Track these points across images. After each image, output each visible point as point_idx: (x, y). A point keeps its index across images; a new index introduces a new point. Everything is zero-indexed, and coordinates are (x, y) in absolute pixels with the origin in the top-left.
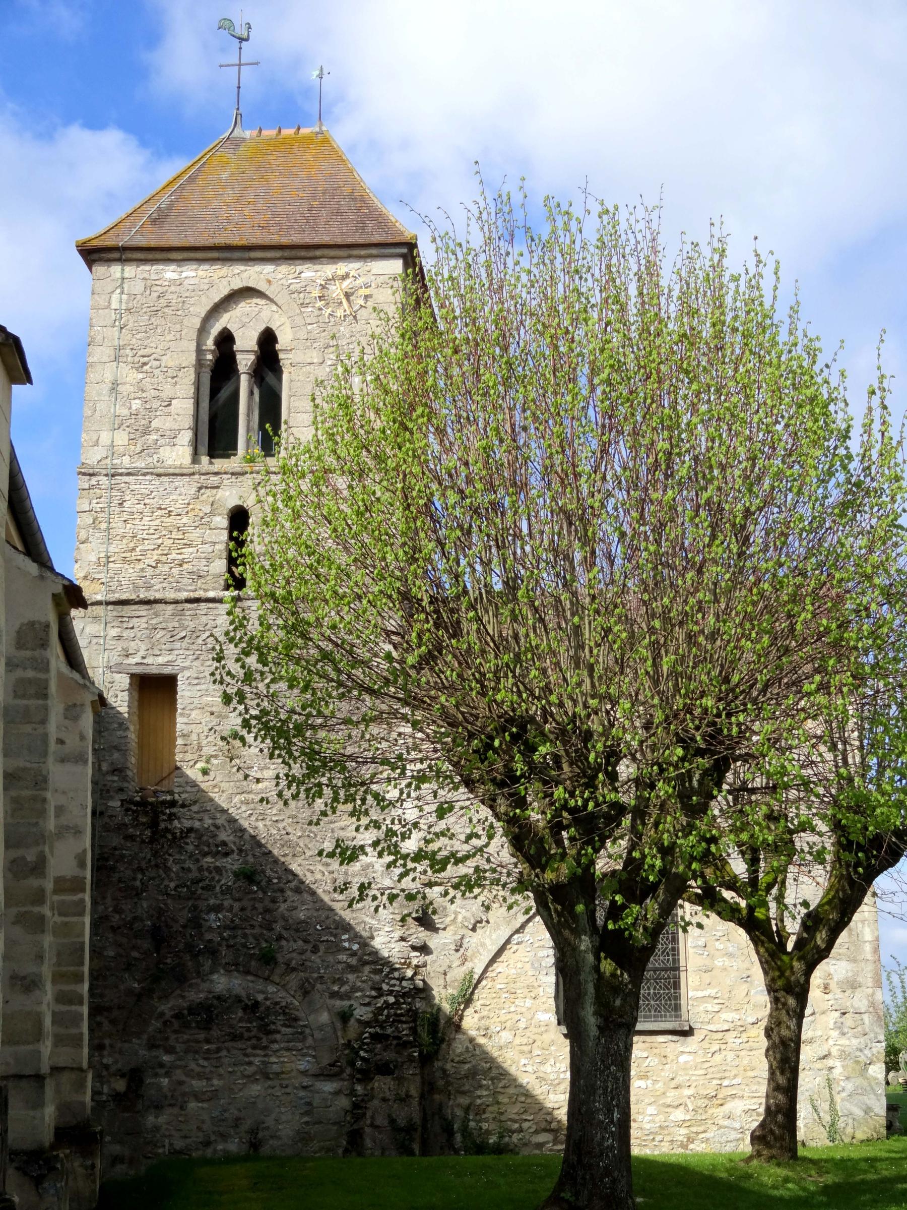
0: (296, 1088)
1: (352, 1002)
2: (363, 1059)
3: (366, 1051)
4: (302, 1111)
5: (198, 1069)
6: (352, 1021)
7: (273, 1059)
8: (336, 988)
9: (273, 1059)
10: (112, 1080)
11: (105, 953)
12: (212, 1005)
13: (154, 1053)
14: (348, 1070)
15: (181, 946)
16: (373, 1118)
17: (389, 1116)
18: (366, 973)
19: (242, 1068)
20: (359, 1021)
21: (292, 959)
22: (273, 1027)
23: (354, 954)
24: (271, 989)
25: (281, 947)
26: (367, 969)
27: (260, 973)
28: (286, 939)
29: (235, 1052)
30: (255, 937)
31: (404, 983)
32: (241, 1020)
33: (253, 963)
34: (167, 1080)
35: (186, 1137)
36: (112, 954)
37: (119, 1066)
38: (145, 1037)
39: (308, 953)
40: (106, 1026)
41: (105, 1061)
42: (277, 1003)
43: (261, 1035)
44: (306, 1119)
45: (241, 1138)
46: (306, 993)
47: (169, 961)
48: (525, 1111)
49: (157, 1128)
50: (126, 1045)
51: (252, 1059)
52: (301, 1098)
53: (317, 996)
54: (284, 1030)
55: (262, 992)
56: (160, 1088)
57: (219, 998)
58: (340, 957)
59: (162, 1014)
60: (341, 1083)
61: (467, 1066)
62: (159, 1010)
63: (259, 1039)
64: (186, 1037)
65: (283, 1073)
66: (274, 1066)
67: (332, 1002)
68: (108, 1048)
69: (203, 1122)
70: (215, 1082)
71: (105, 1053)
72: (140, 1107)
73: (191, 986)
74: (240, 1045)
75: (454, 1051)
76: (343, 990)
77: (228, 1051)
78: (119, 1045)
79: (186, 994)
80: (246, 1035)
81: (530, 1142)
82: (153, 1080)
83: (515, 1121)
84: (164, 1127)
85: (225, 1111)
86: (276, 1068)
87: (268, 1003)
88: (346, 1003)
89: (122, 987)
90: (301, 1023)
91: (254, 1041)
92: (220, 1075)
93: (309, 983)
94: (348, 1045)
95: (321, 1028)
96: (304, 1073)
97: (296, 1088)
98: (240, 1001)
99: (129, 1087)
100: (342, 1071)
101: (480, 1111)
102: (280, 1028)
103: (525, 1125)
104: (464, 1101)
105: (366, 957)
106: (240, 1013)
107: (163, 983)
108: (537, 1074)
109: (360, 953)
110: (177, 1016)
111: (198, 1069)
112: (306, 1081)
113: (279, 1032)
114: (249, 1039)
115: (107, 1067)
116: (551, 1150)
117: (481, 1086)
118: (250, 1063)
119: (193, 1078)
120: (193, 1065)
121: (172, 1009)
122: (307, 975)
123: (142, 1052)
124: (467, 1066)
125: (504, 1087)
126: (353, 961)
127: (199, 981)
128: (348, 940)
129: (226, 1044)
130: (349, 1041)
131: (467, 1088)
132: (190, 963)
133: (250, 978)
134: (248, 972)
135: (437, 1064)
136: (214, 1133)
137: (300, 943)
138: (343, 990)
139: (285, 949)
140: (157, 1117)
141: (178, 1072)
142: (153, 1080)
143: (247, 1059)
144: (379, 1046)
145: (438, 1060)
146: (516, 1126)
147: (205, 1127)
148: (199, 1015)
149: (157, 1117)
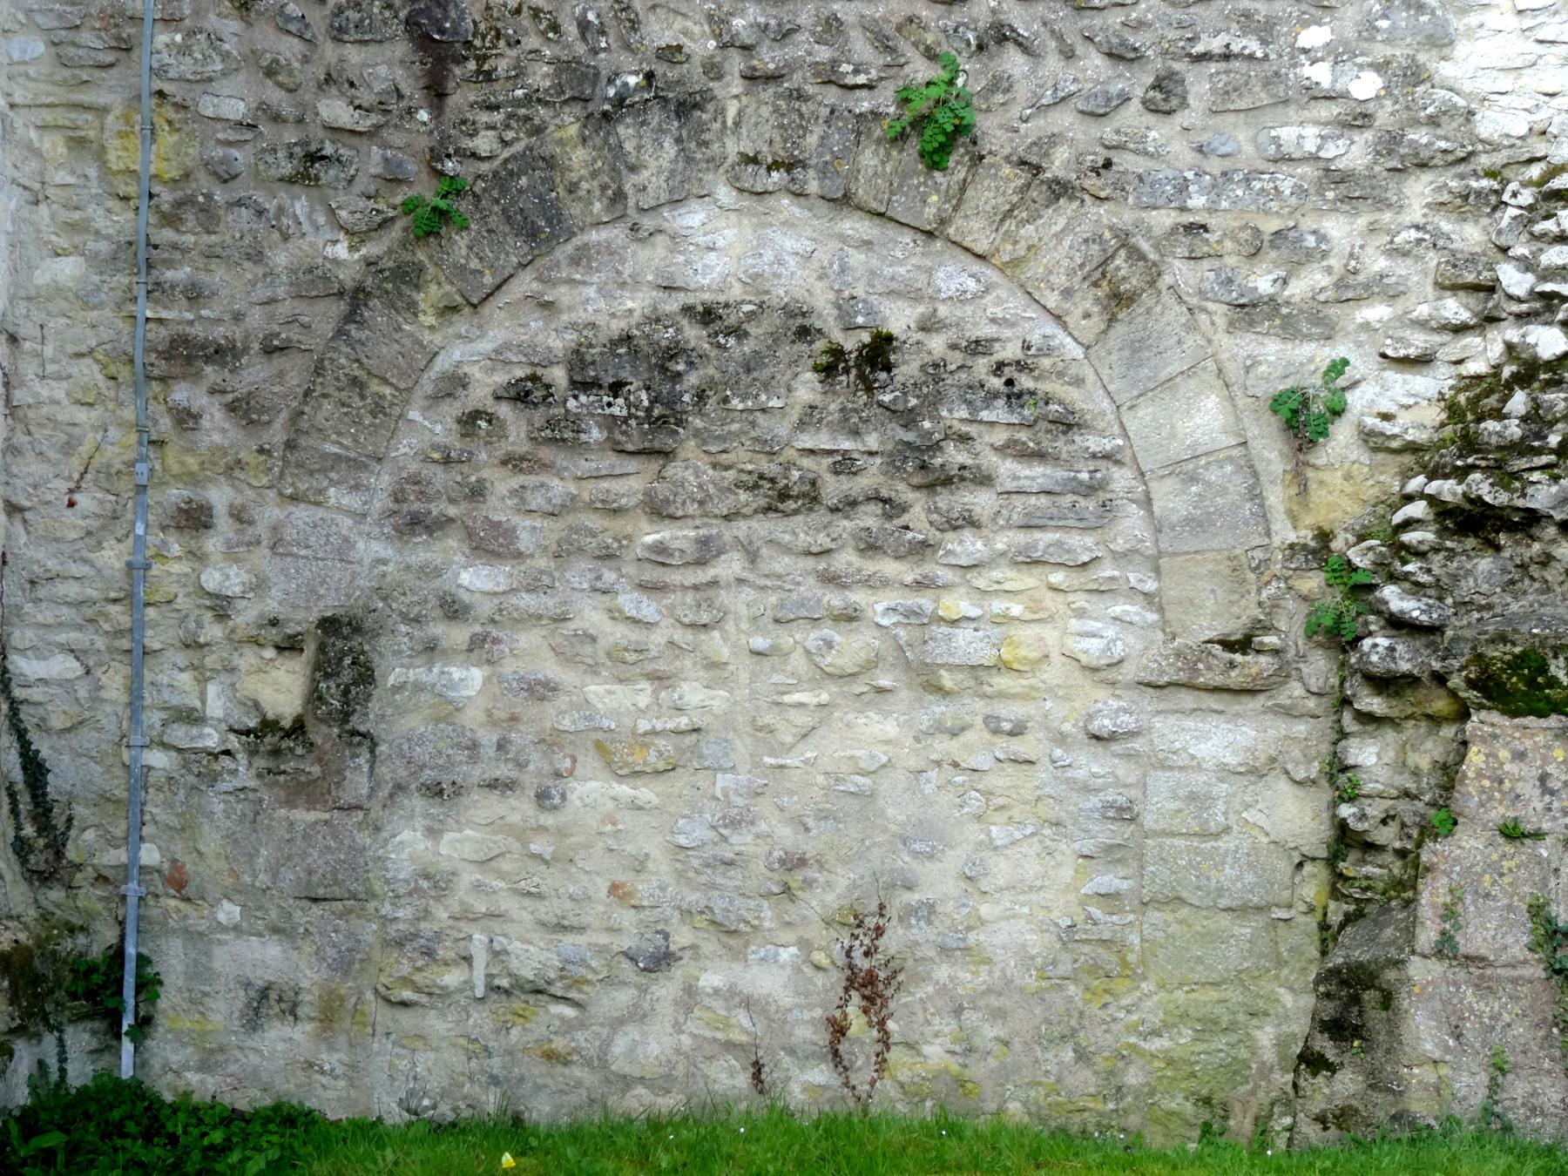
0: (1061, 739)
1: (1340, 350)
2: (1398, 624)
3: (1418, 588)
4: (1088, 846)
5: (619, 633)
6: (1342, 434)
7: (957, 604)
8: (1263, 283)
9: (957, 604)
10: (247, 659)
11: (208, 107)
12: (673, 352)
13: (423, 552)
14: (1319, 667)
15: (540, 76)
16: (1449, 913)
17: (1537, 911)
18: (1416, 213)
19: (812, 638)
20: (1373, 441)
21: (1054, 139)
22: (954, 456)
23: (1359, 119)
24: (953, 277)
25: (1000, 84)
26: (1419, 191)
27: (898, 212)
28: (1024, 47)
29: (782, 564)
30: (884, 45)
32: (810, 418)
33: (869, 158)
34: (477, 675)
35: (562, 928)
36: (236, 109)
37: (272, 604)
38: (382, 481)
39: (1132, 116)
40: (217, 427)
41: (212, 580)
42: (977, 347)
43: (906, 495)
44: (1107, 881)
45: (805, 945)
46: (1119, 300)
47: (484, 143)
49: (435, 882)
50: (302, 513)
51: (858, 597)
52: (1087, 789)
53: (1174, 314)
54: (1008, 470)
55: (914, 296)
56: (447, 710)
57: (707, 316)
58: (1287, 134)
59: (456, 383)
60: (1279, 728)
62: (442, 364)
63: (891, 507)
64: (559, 488)
65: (1002, 667)
66: (963, 636)
67: (1237, 347)
68: (223, 522)
69: (640, 865)
70: (693, 693)
71: (212, 544)
72: (357, 783)
73: (580, 258)
74: (800, 530)
76: (1298, 289)
77: (753, 557)
78: (270, 512)
79: (562, 294)
80: (833, 488)
82: (417, 673)
84: (468, 877)
85: (735, 824)
86: (968, 645)
87: (937, 344)
88: (1312, 356)
89: (280, 258)
90: (1094, 443)
91: (869, 518)
92: (714, 665)
93: (1136, 255)
94: (1320, 549)
95: (1185, 470)
96: (1101, 672)
97: (1061, 739)
98: (804, 333)
99: (315, 697)
100: (1283, 675)
102: (990, 460)
105: (1421, 136)
106: (807, 388)
107: (461, 241)
109: (1384, 117)
110: (521, 394)
111: (619, 633)
112: (1110, 712)
113: (984, 480)
114: (849, 505)
115: (221, 606)
118: (849, 617)
119: (593, 669)
120: (591, 616)
121: (497, 358)
122: (1126, 217)
123: (373, 548)
126: (1354, 153)
127: (616, 234)
128: (1338, 54)
129: (741, 528)
130: (1324, 537)
132: (579, 157)
133: (855, 226)
134: (844, 201)
136: (686, 914)
137: (1094, 63)
138: (1298, 289)
139: (1022, 92)
140: (433, 833)
141: (528, 639)
142: (417, 673)
143: (835, 599)
144: (1485, 564)
147: (644, 888)
148: (616, 388)
149: (433, 833)
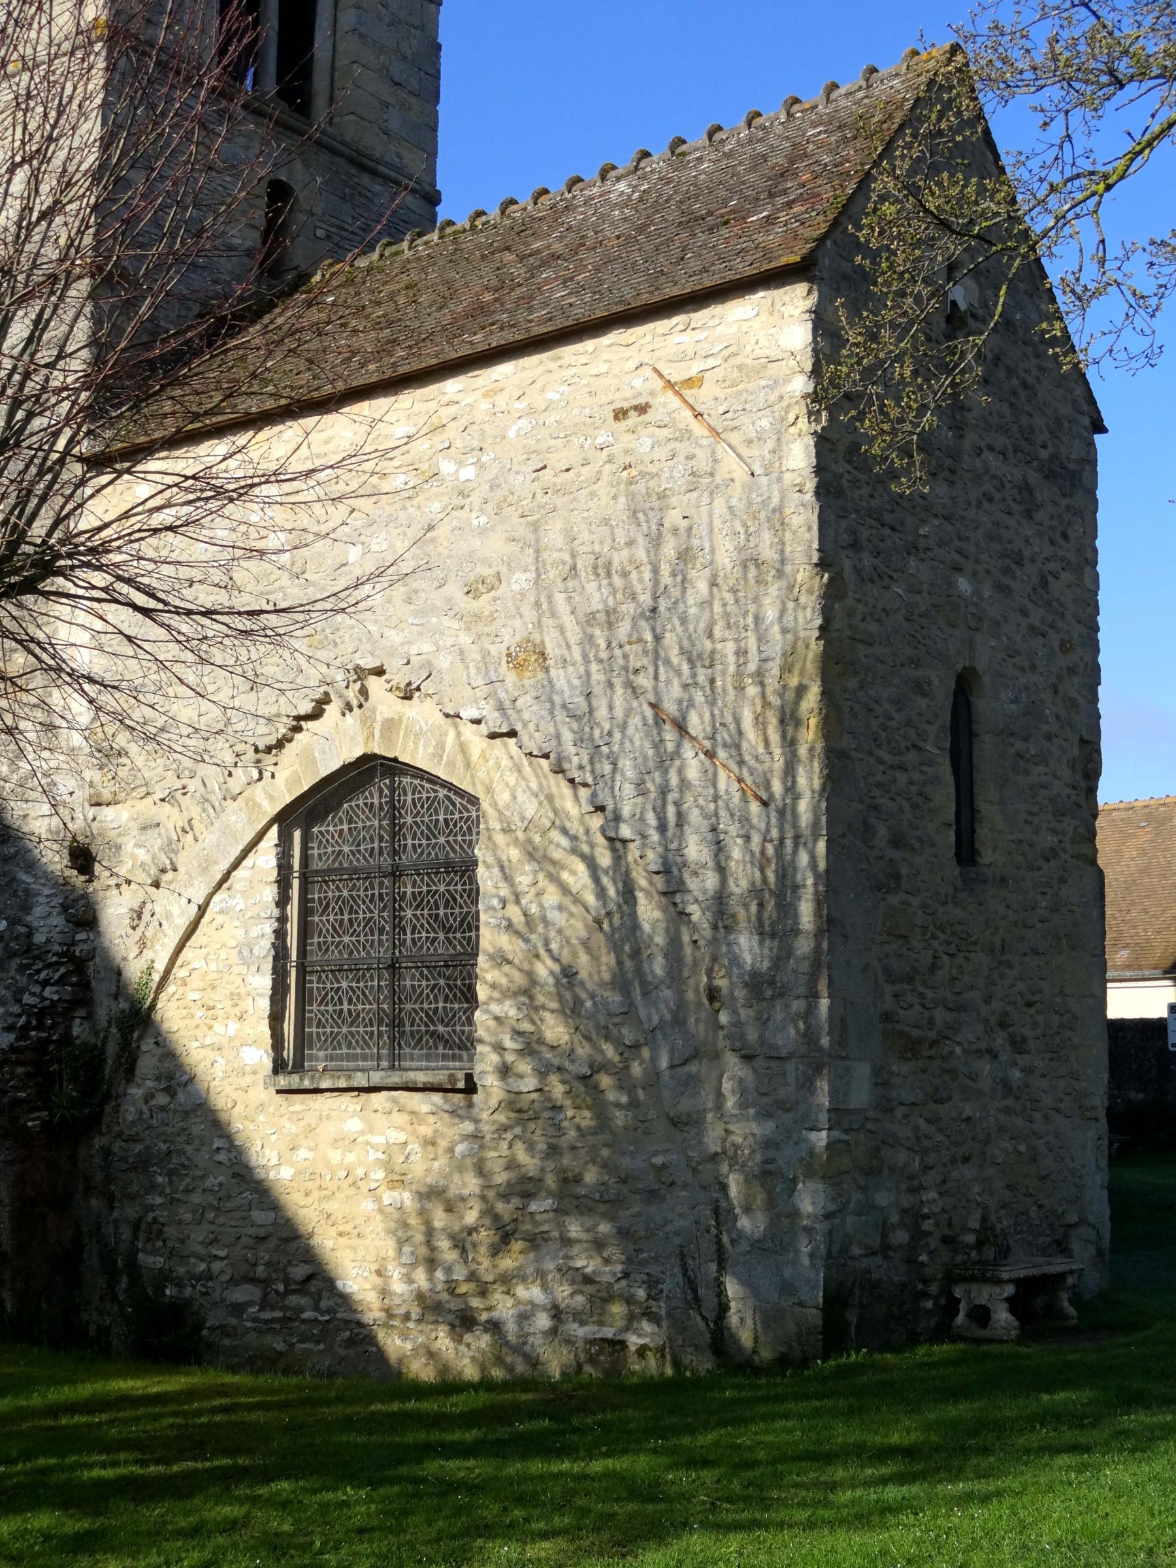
31: (48, 991)
48: (215, 1240)
61: (138, 1147)
75: (125, 1120)
81: (223, 1300)
83: (203, 1260)
101: (155, 1232)
103: (216, 1266)
104: (131, 1211)
108: (236, 1169)
116: (255, 1320)
117: (153, 1187)
124: (138, 1147)
125: (187, 1191)
131: (135, 1188)
135: (99, 1142)
145: (101, 1134)
146: (203, 1266)
